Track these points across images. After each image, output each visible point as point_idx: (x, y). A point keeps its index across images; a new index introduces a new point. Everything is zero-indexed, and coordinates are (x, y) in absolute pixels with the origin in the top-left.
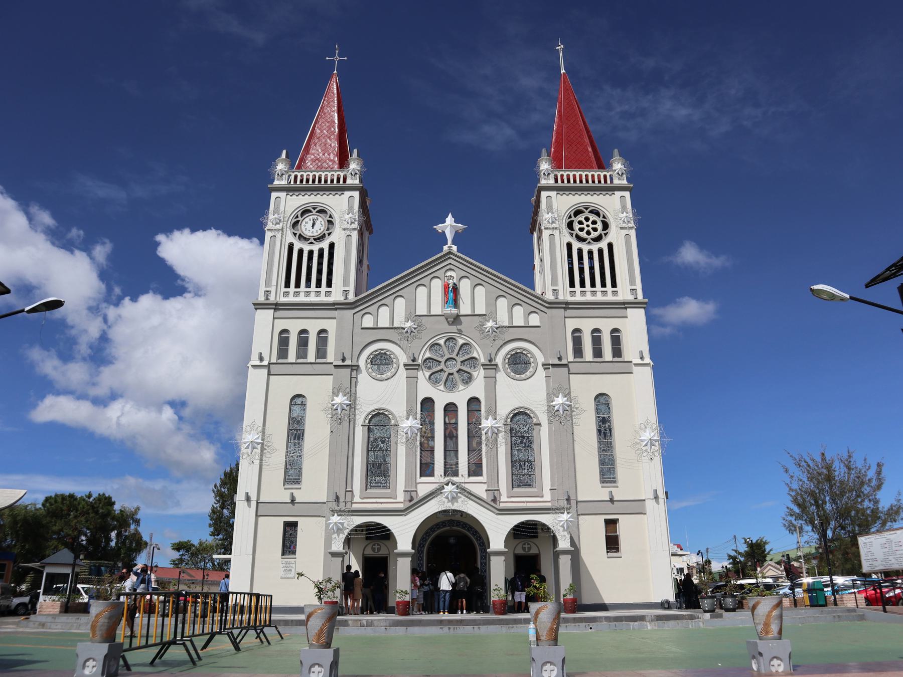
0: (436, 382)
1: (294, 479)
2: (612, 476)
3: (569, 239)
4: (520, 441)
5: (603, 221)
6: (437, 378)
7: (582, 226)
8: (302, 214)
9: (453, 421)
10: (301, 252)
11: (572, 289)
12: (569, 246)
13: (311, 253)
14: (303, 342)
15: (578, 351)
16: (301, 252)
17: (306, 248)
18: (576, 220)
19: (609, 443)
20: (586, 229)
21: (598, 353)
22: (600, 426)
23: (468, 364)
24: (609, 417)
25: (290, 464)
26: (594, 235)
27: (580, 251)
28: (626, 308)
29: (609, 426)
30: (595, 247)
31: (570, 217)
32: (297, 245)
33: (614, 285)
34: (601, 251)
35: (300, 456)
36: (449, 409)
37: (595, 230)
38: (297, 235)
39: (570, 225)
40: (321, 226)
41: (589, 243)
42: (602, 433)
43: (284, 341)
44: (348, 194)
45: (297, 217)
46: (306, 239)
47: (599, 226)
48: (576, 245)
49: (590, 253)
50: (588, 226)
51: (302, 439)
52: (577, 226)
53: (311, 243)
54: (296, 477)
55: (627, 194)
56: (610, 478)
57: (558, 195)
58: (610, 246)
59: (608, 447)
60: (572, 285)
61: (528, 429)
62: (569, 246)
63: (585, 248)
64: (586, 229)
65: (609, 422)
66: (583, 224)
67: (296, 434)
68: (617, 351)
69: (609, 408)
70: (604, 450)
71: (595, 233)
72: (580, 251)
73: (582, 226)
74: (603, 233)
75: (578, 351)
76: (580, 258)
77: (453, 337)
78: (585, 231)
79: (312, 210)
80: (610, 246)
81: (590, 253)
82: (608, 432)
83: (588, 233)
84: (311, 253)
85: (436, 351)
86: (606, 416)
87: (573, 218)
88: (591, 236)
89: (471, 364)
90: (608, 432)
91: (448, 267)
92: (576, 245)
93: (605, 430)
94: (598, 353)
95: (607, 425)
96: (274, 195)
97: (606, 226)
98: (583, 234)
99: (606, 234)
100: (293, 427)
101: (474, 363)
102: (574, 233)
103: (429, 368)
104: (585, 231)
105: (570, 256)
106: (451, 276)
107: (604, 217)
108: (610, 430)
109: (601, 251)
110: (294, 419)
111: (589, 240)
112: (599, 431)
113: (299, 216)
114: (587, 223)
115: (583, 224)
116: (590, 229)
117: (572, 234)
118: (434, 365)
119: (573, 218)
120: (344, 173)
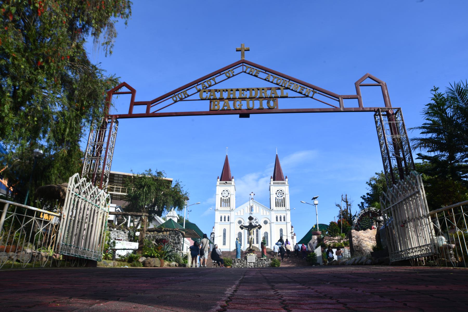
10: (223, 199)
12: (276, 198)
13: (225, 200)
14: (225, 218)
16: (223, 199)
18: (277, 192)
26: (281, 196)
33: (284, 206)
39: (276, 194)
40: (227, 193)
55: (288, 186)
62: (276, 198)
63: (279, 198)
80: (284, 198)
84: (225, 200)
92: (277, 198)
96: (217, 187)
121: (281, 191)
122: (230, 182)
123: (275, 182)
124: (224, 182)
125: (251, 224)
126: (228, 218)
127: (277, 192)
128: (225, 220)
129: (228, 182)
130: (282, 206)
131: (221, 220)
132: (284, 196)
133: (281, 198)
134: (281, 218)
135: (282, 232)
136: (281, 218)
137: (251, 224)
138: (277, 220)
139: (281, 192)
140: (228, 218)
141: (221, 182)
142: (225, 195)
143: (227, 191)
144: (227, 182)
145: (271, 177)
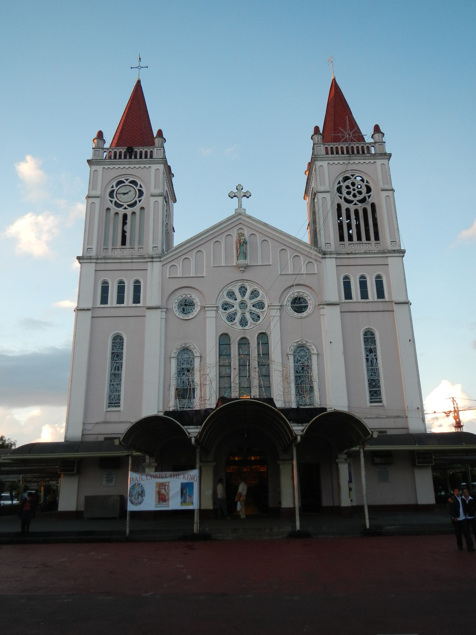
0: (231, 321)
1: (115, 403)
2: (378, 397)
3: (338, 200)
4: (301, 368)
6: (232, 318)
7: (349, 190)
9: (246, 353)
11: (342, 243)
12: (339, 206)
15: (348, 295)
17: (121, 211)
18: (344, 185)
19: (375, 370)
20: (353, 192)
21: (364, 295)
22: (367, 356)
23: (257, 306)
24: (375, 348)
25: (111, 391)
26: (360, 197)
27: (348, 210)
28: (387, 257)
29: (375, 355)
30: (360, 207)
31: (339, 183)
33: (377, 238)
34: (365, 210)
35: (120, 384)
36: (244, 342)
38: (113, 202)
39: (339, 190)
41: (355, 204)
42: (369, 361)
43: (105, 289)
44: (154, 167)
45: (113, 187)
46: (120, 206)
48: (345, 206)
49: (356, 212)
50: (354, 190)
51: (121, 370)
52: (344, 191)
53: (125, 208)
54: (117, 402)
56: (377, 399)
57: (329, 164)
58: (373, 206)
59: (375, 373)
60: (342, 239)
61: (308, 358)
62: (339, 206)
64: (353, 192)
65: (376, 352)
66: (350, 188)
67: (116, 366)
68: (380, 294)
69: (375, 341)
70: (372, 375)
71: (360, 195)
72: (348, 210)
73: (349, 190)
74: (367, 195)
76: (348, 217)
77: (244, 283)
78: (352, 194)
79: (125, 181)
81: (356, 212)
82: (375, 360)
83: (354, 196)
85: (231, 295)
86: (372, 347)
87: (342, 184)
88: (356, 198)
89: (260, 305)
90: (375, 360)
91: (240, 226)
92: (345, 206)
93: (372, 359)
94: (364, 295)
95: (373, 354)
97: (369, 189)
98: (350, 197)
99: (369, 197)
100: (113, 360)
101: (262, 305)
103: (225, 309)
104: (352, 194)
105: (339, 215)
106: (242, 233)
107: (367, 182)
108: (376, 359)
109: (365, 210)
110: (114, 354)
111: (355, 201)
112: (367, 360)
113: (114, 186)
114: (354, 187)
115: (350, 188)
116: (356, 192)
117: (341, 197)
118: (230, 307)
119: (342, 184)
120: (151, 149)
123: (334, 145)
126: (137, 289)
127: (344, 185)
128: (121, 300)
129: (138, 150)
130: (368, 238)
131: (104, 300)
132: (370, 200)
133: (360, 207)
135: (374, 342)
138: (348, 295)
140: (137, 289)
142: (124, 200)
144: (138, 150)
145: (317, 129)
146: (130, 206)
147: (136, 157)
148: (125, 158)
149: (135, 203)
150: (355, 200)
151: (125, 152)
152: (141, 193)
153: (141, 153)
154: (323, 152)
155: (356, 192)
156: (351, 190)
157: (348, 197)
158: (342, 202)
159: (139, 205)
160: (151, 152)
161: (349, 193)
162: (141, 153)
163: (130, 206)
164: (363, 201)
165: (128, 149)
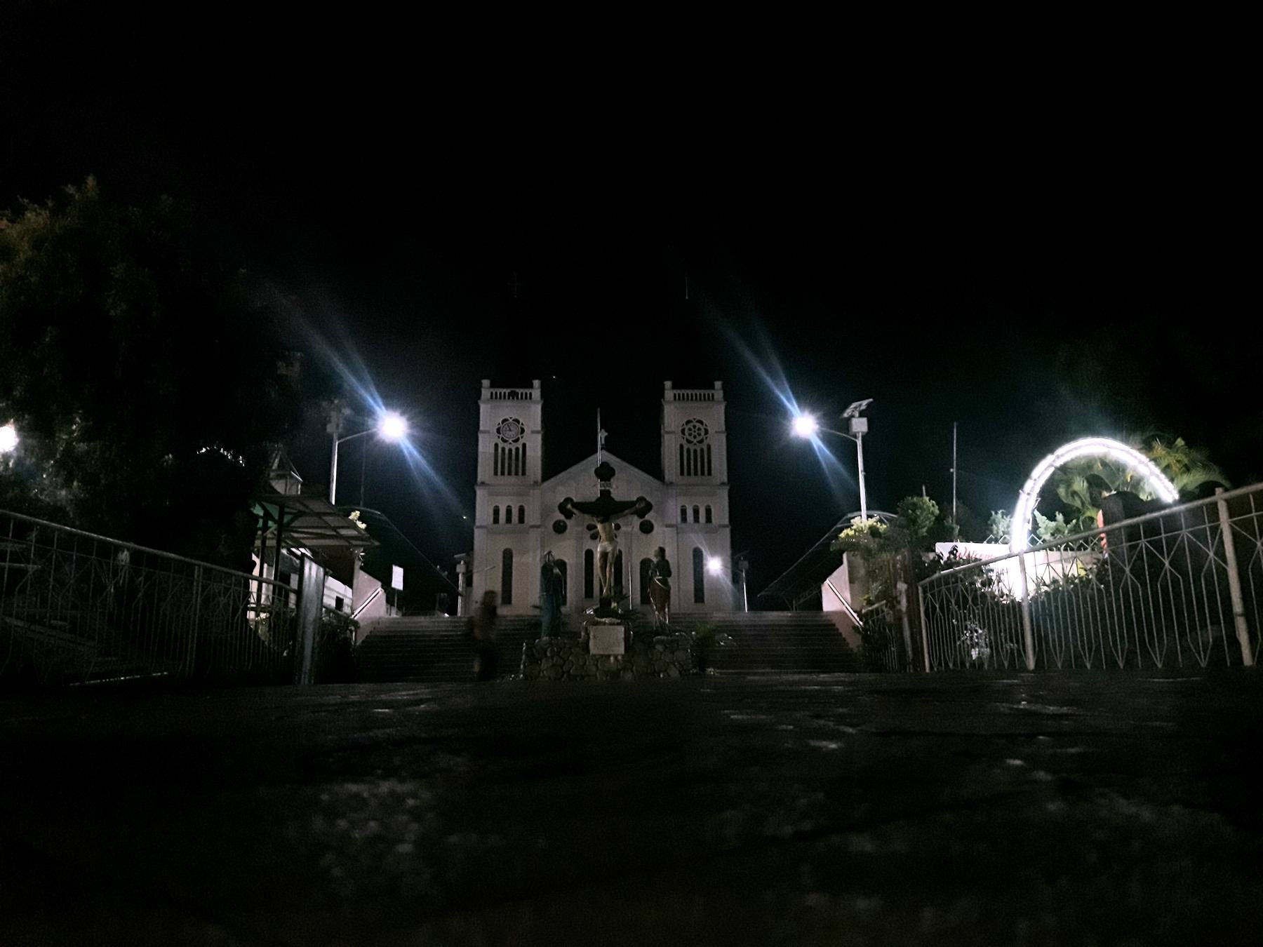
5: (705, 429)
8: (502, 423)
12: (682, 446)
15: (684, 519)
21: (696, 519)
26: (699, 438)
27: (688, 450)
32: (501, 445)
37: (699, 435)
47: (703, 432)
49: (695, 451)
50: (695, 432)
58: (709, 447)
64: (696, 434)
75: (684, 519)
81: (695, 451)
94: (696, 519)
97: (706, 432)
98: (691, 438)
102: (685, 437)
109: (702, 450)
121: (701, 422)
122: (528, 391)
124: (507, 391)
125: (605, 494)
129: (520, 391)
131: (496, 520)
132: (706, 442)
134: (696, 512)
136: (696, 512)
137: (605, 494)
139: (694, 429)
141: (494, 391)
143: (518, 422)
146: (514, 441)
147: (518, 398)
148: (509, 398)
149: (516, 441)
150: (695, 441)
151: (509, 393)
152: (523, 431)
153: (522, 394)
154: (672, 399)
155: (696, 434)
156: (692, 432)
157: (689, 438)
158: (684, 442)
159: (521, 441)
160: (531, 394)
161: (690, 435)
162: (522, 394)
163: (514, 441)
164: (701, 442)
165: (512, 392)
